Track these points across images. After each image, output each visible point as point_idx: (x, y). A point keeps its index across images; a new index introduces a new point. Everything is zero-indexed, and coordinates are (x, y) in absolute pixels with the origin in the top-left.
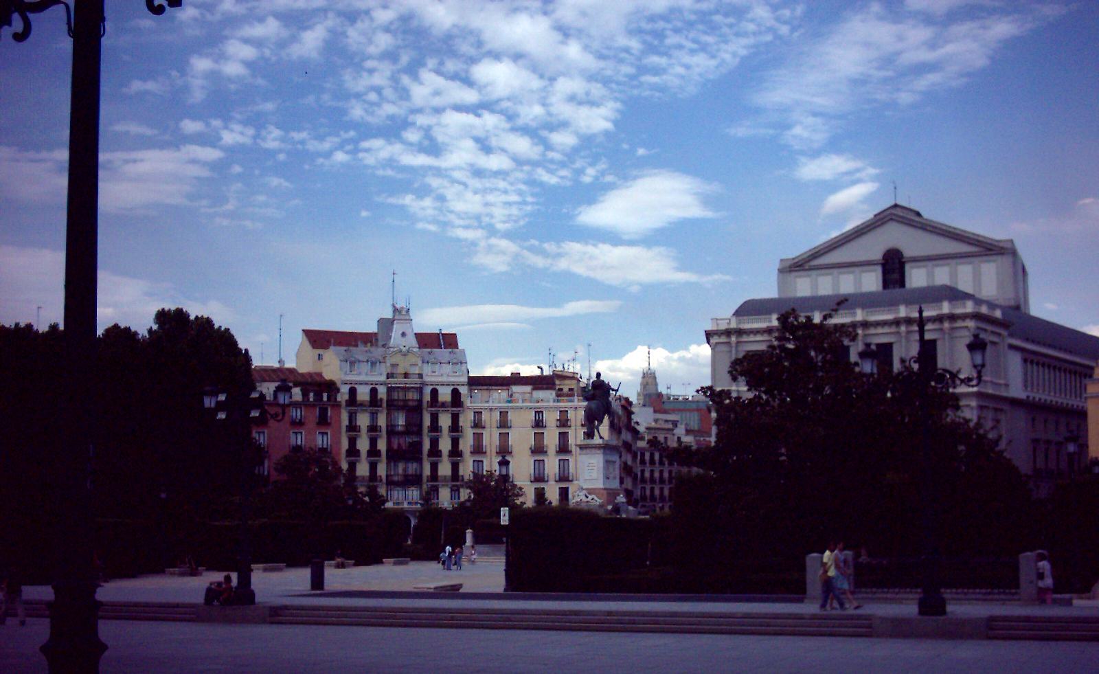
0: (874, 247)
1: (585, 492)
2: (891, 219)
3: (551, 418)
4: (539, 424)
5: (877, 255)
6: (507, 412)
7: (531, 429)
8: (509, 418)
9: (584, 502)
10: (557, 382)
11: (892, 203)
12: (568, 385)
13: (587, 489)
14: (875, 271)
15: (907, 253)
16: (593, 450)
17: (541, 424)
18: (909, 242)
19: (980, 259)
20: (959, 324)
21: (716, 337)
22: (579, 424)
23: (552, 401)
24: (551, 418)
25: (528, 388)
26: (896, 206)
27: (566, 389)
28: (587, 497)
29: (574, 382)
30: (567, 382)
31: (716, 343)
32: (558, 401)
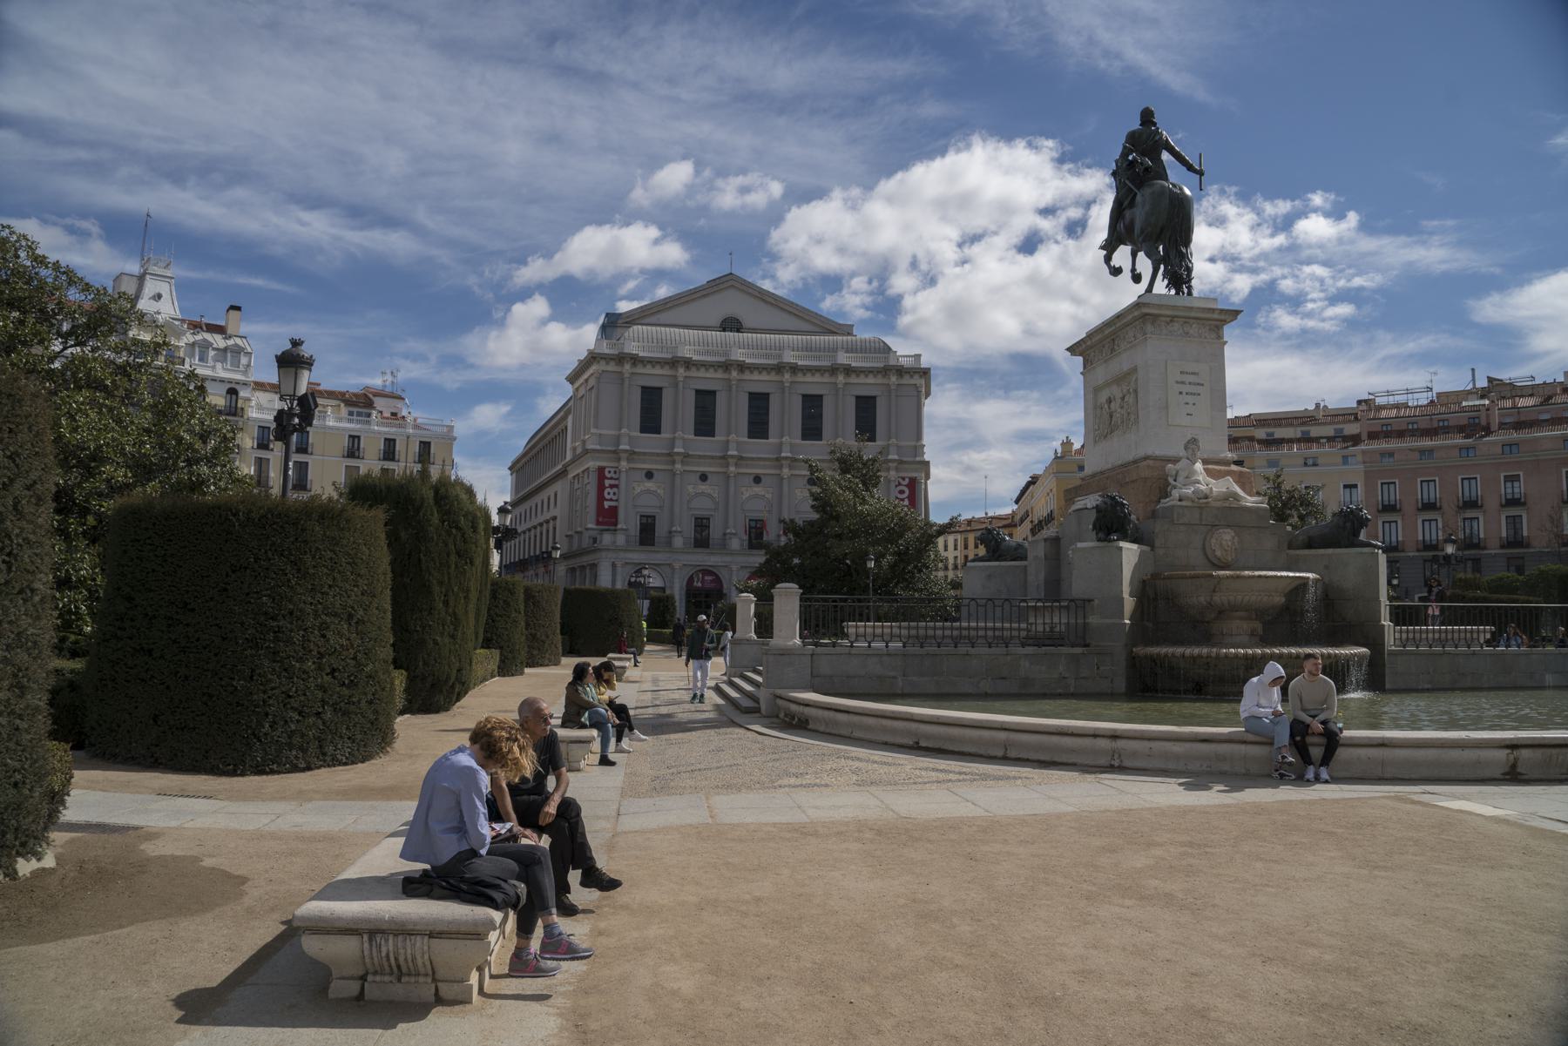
8: (310, 441)
17: (357, 454)
20: (906, 380)
25: (334, 402)
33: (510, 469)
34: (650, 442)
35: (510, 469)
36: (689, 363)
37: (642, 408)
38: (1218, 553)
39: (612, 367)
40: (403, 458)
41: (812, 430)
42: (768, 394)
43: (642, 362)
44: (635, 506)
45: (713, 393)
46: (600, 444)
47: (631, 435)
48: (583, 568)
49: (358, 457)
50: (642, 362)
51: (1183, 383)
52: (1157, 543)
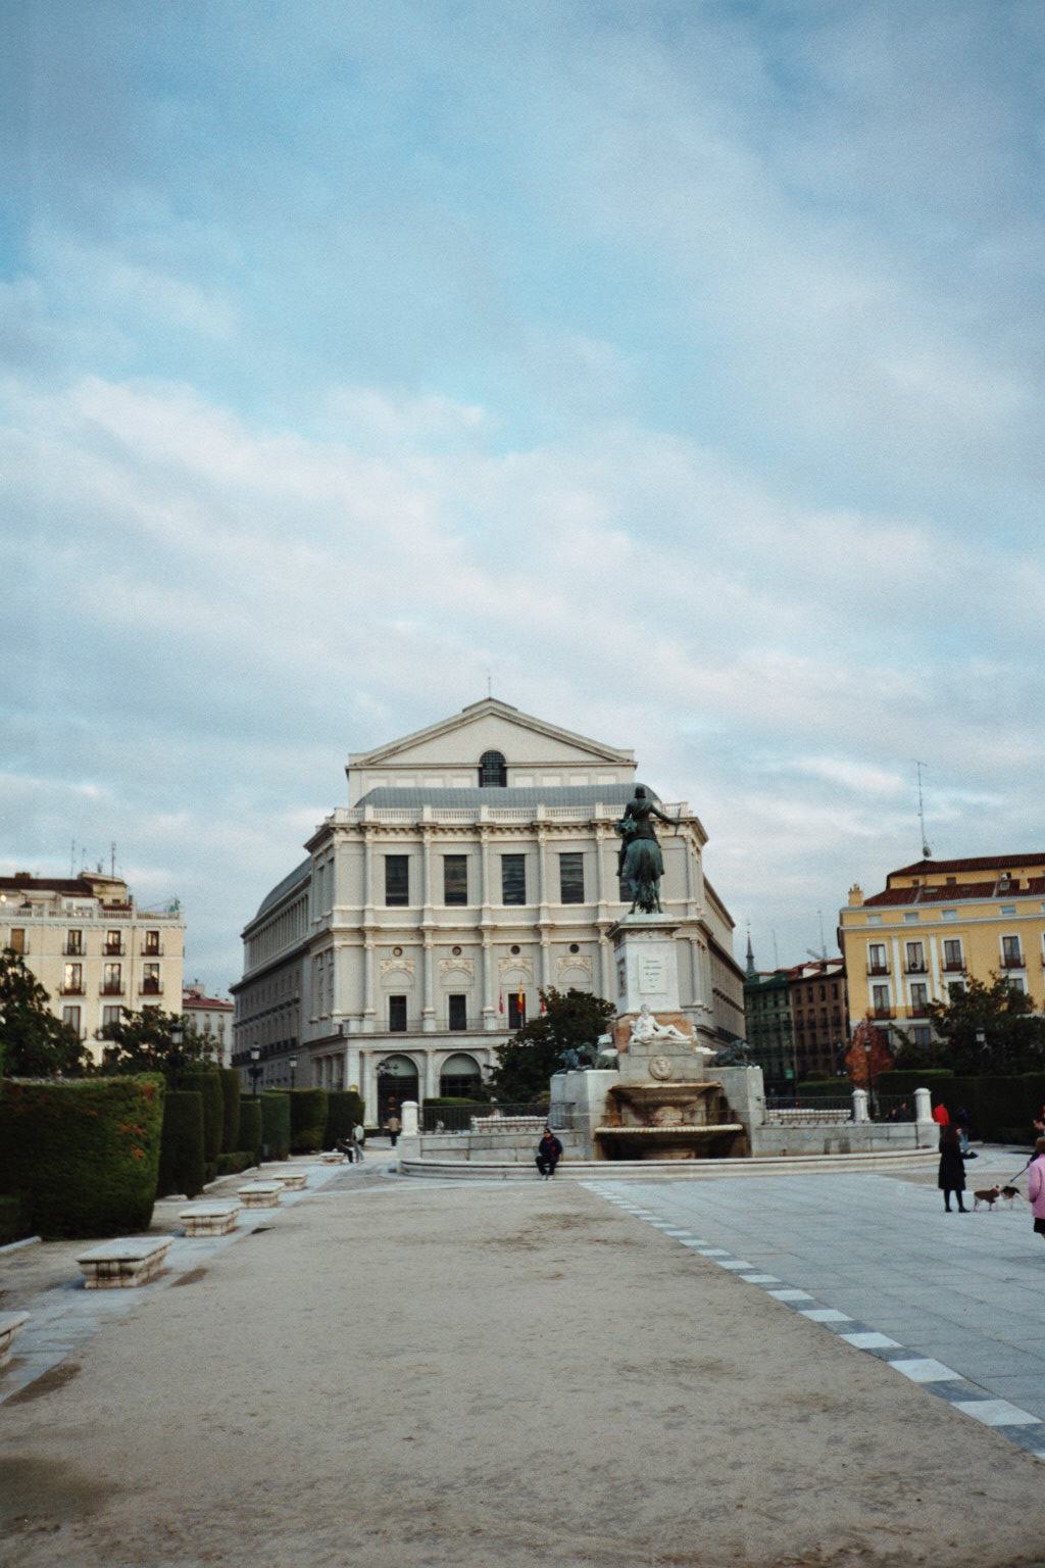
0: (470, 746)
1: (651, 1020)
2: (492, 714)
3: (95, 941)
4: (73, 950)
5: (474, 757)
6: (23, 931)
7: (101, 957)
8: (27, 939)
9: (658, 1039)
10: (96, 888)
11: (487, 697)
12: (114, 894)
13: (655, 1014)
14: (471, 776)
15: (511, 757)
16: (655, 935)
17: (78, 949)
18: (515, 746)
19: (599, 770)
21: (342, 833)
22: (138, 951)
23: (95, 915)
24: (95, 941)
25: (51, 894)
26: (490, 700)
27: (108, 901)
28: (657, 1030)
29: (120, 889)
30: (112, 889)
31: (344, 842)
32: (106, 916)
33: (243, 936)
34: (398, 918)
35: (243, 936)
36: (434, 827)
37: (387, 878)
38: (658, 1072)
39: (353, 837)
40: (128, 953)
41: (572, 893)
42: (523, 855)
43: (384, 829)
44: (384, 987)
45: (464, 858)
46: (343, 921)
47: (377, 902)
48: (329, 1058)
49: (80, 954)
50: (384, 829)
51: (648, 968)
52: (621, 1067)
